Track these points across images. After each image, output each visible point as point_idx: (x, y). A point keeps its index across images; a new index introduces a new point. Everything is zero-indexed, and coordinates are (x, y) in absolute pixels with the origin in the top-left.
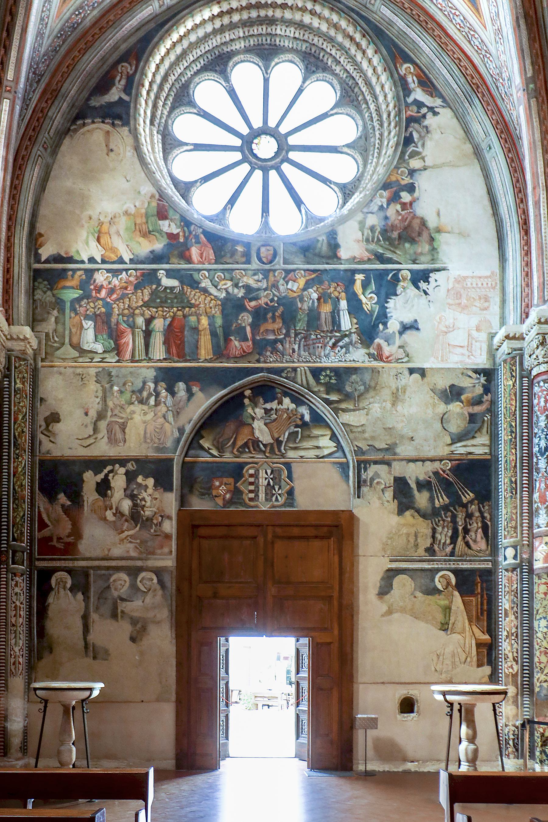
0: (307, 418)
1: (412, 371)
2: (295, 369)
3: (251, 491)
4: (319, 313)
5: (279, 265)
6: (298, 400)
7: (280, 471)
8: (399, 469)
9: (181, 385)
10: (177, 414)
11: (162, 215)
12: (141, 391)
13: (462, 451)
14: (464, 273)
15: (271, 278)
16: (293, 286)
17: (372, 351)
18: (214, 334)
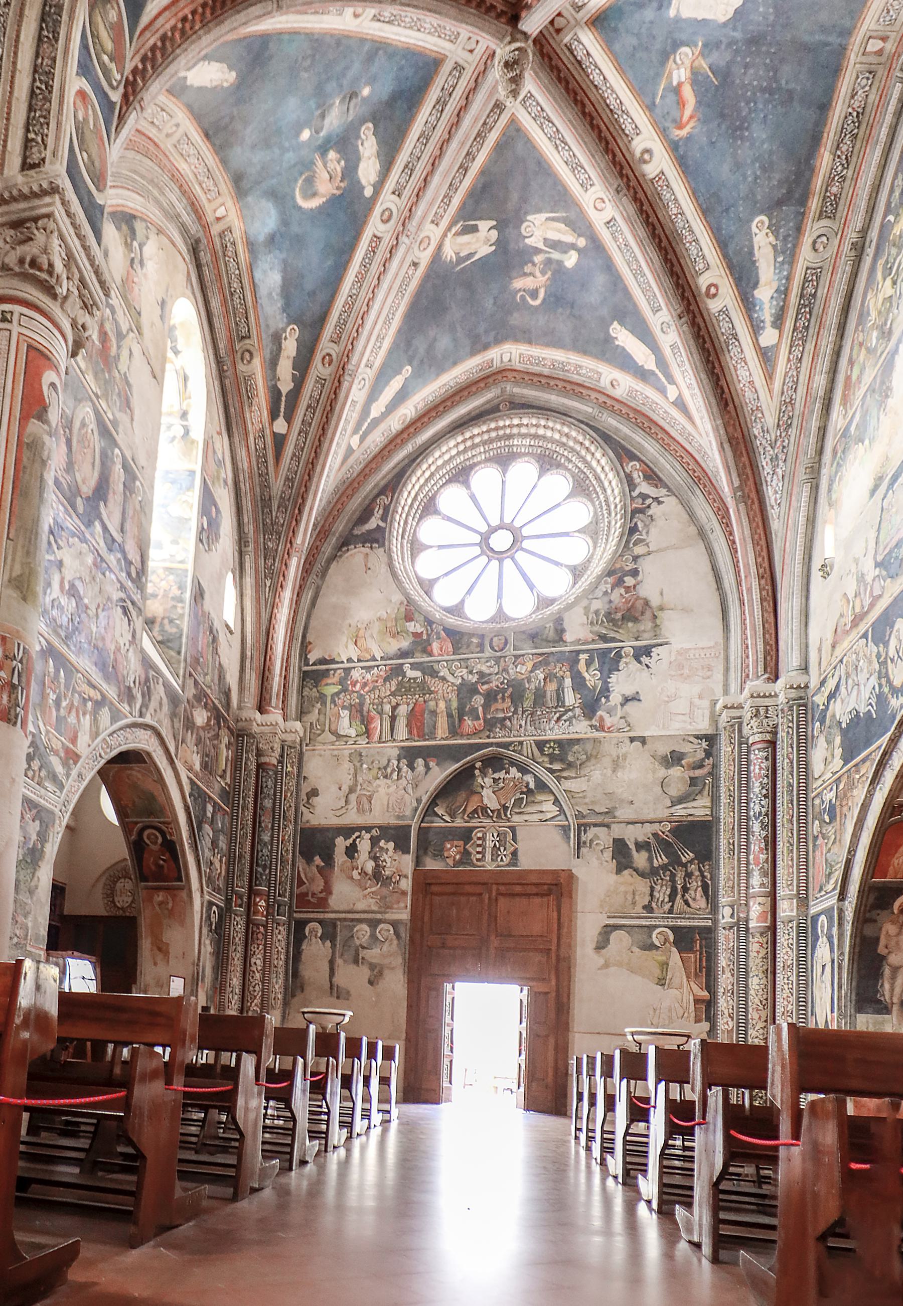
0: (532, 785)
1: (632, 739)
2: (521, 743)
3: (478, 853)
4: (545, 692)
5: (510, 651)
6: (524, 770)
7: (505, 834)
8: (617, 831)
9: (420, 761)
10: (416, 786)
11: (409, 618)
12: (385, 768)
13: (683, 812)
14: (687, 646)
15: (502, 664)
16: (523, 670)
17: (594, 722)
18: (450, 715)
